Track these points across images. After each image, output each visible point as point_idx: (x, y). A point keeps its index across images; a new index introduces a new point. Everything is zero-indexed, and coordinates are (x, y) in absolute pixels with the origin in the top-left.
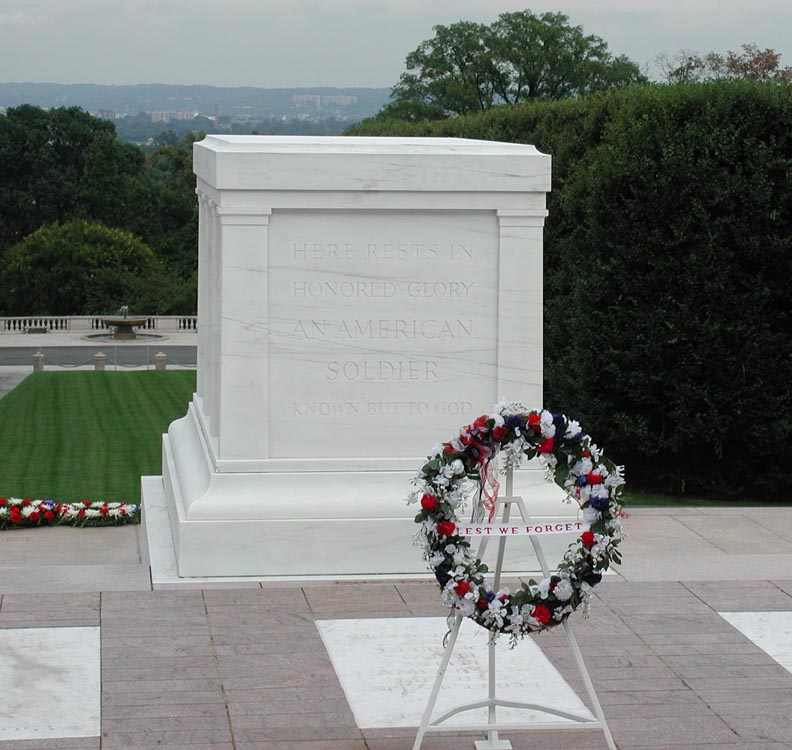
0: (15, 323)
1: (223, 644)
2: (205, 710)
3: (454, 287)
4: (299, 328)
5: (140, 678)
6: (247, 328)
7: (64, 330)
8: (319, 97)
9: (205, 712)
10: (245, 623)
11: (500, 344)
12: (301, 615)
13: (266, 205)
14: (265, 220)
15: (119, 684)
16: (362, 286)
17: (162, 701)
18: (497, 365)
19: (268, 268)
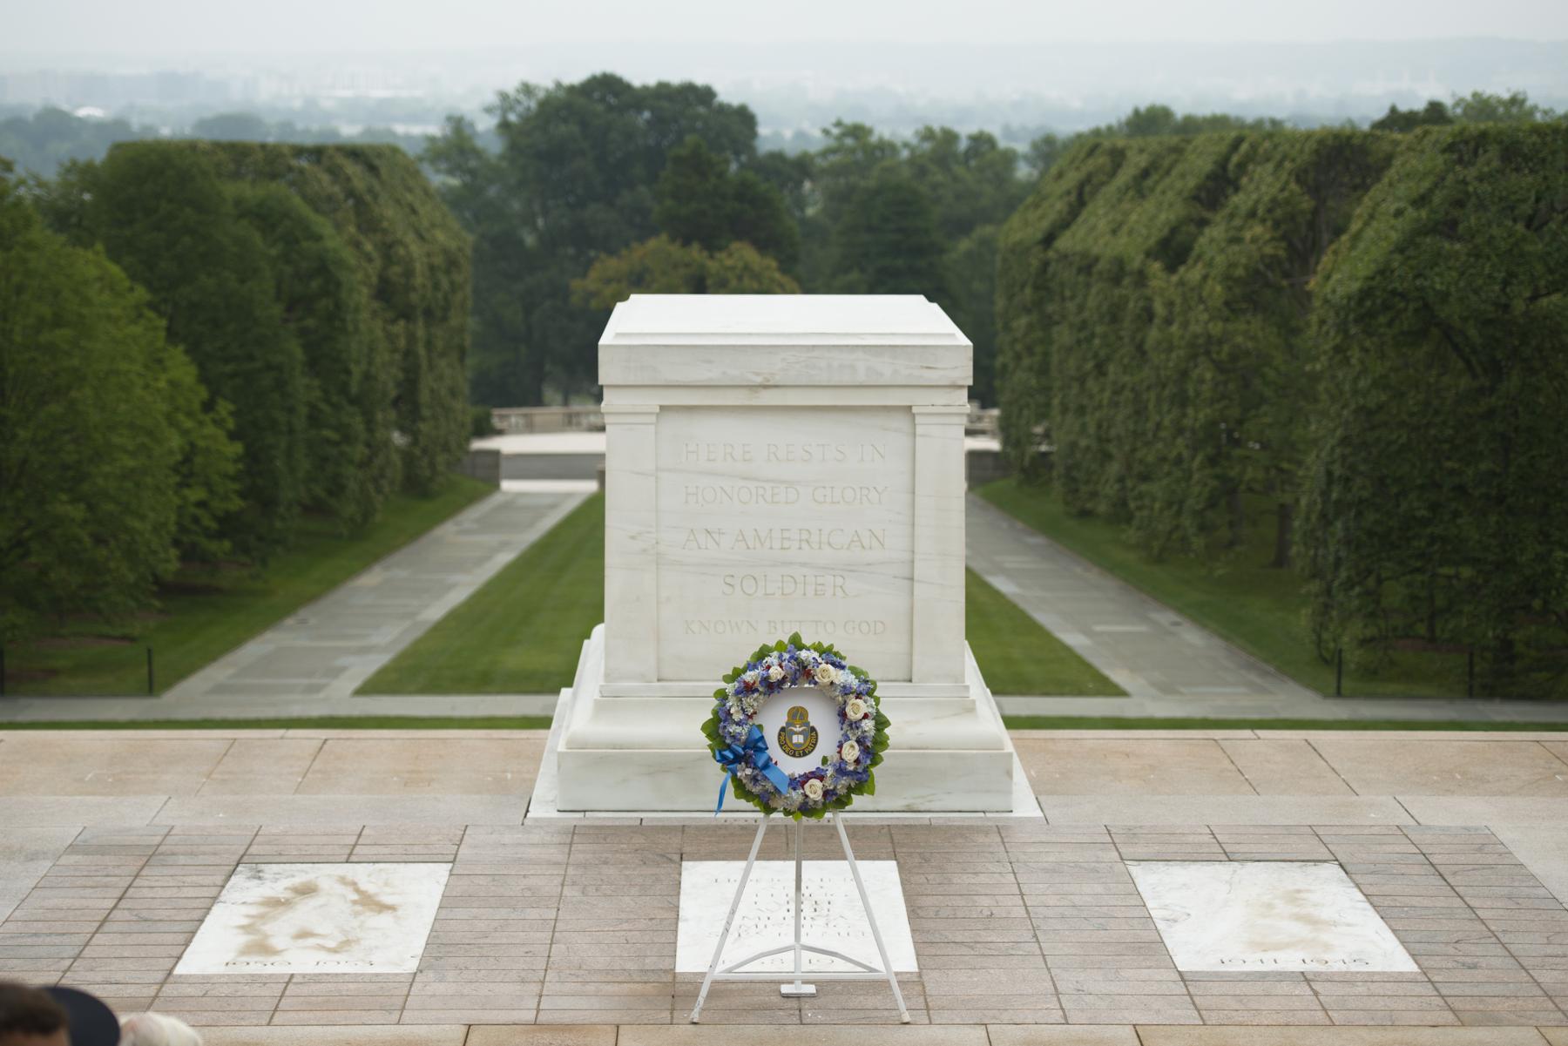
1: (574, 883)
2: (527, 950)
3: (865, 492)
4: (692, 538)
5: (475, 918)
6: (633, 538)
9: (527, 953)
10: (605, 863)
11: (917, 557)
12: (668, 856)
13: (654, 401)
14: (653, 419)
16: (761, 491)
17: (487, 941)
18: (912, 579)
19: (657, 469)
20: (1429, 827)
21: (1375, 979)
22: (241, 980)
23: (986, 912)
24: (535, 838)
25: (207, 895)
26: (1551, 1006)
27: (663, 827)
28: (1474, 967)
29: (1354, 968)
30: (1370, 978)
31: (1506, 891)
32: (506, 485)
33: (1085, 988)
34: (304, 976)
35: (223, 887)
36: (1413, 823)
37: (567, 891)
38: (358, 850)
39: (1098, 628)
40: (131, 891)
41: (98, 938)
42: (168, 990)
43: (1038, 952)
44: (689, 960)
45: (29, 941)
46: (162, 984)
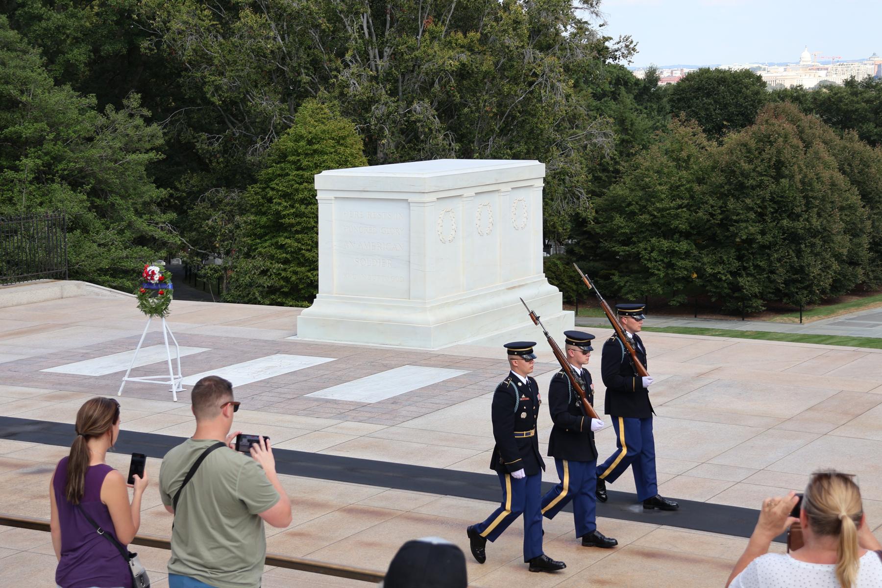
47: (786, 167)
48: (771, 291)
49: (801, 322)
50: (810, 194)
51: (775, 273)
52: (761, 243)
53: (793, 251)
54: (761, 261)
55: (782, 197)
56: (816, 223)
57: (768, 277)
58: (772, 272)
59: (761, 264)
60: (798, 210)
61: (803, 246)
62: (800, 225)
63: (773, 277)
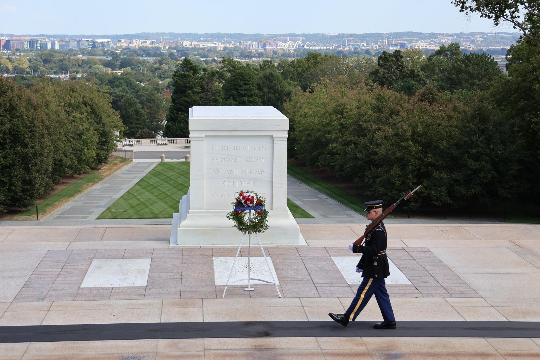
0: (154, 141)
1: (185, 263)
5: (160, 272)
7: (174, 144)
8: (288, 38)
10: (193, 258)
13: (203, 134)
15: (154, 273)
17: (164, 278)
18: (273, 182)
20: (411, 247)
21: (400, 285)
22: (99, 289)
23: (296, 269)
24: (173, 252)
25: (86, 267)
26: (447, 292)
27: (206, 249)
28: (426, 282)
29: (394, 283)
30: (398, 286)
31: (432, 264)
32: (134, 160)
33: (324, 288)
34: (116, 287)
35: (90, 265)
36: (406, 246)
37: (184, 265)
38: (125, 255)
39: (304, 200)
40: (64, 267)
41: (58, 279)
42: (80, 292)
43: (311, 279)
44: (219, 282)
45: (39, 280)
46: (78, 290)
47: (16, 110)
48: (10, 198)
49: (37, 219)
50: (33, 129)
51: (13, 185)
52: (4, 165)
53: (22, 169)
54: (3, 178)
55: (17, 131)
56: (39, 149)
57: (9, 189)
58: (11, 184)
59: (4, 179)
60: (27, 140)
61: (30, 165)
62: (29, 151)
63: (13, 188)
